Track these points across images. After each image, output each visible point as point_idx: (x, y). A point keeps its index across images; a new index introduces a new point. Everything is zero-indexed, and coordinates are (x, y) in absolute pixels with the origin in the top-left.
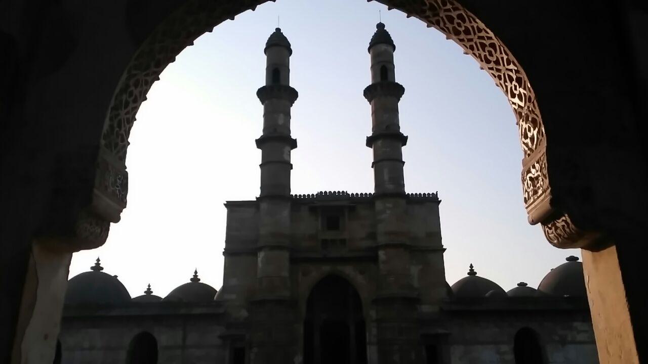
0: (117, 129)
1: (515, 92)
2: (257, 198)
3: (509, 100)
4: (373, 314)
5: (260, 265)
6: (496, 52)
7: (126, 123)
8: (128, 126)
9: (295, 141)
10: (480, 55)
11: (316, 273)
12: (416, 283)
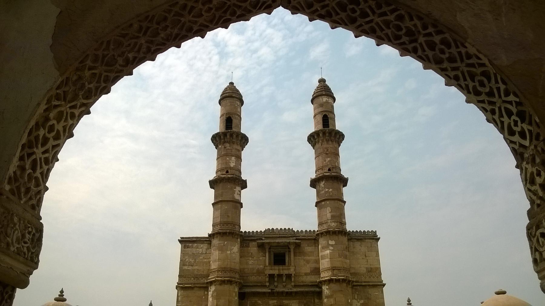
0: (30, 171)
1: (515, 128)
2: (210, 235)
3: (505, 138)
6: (489, 81)
7: (43, 163)
8: (45, 168)
10: (467, 86)
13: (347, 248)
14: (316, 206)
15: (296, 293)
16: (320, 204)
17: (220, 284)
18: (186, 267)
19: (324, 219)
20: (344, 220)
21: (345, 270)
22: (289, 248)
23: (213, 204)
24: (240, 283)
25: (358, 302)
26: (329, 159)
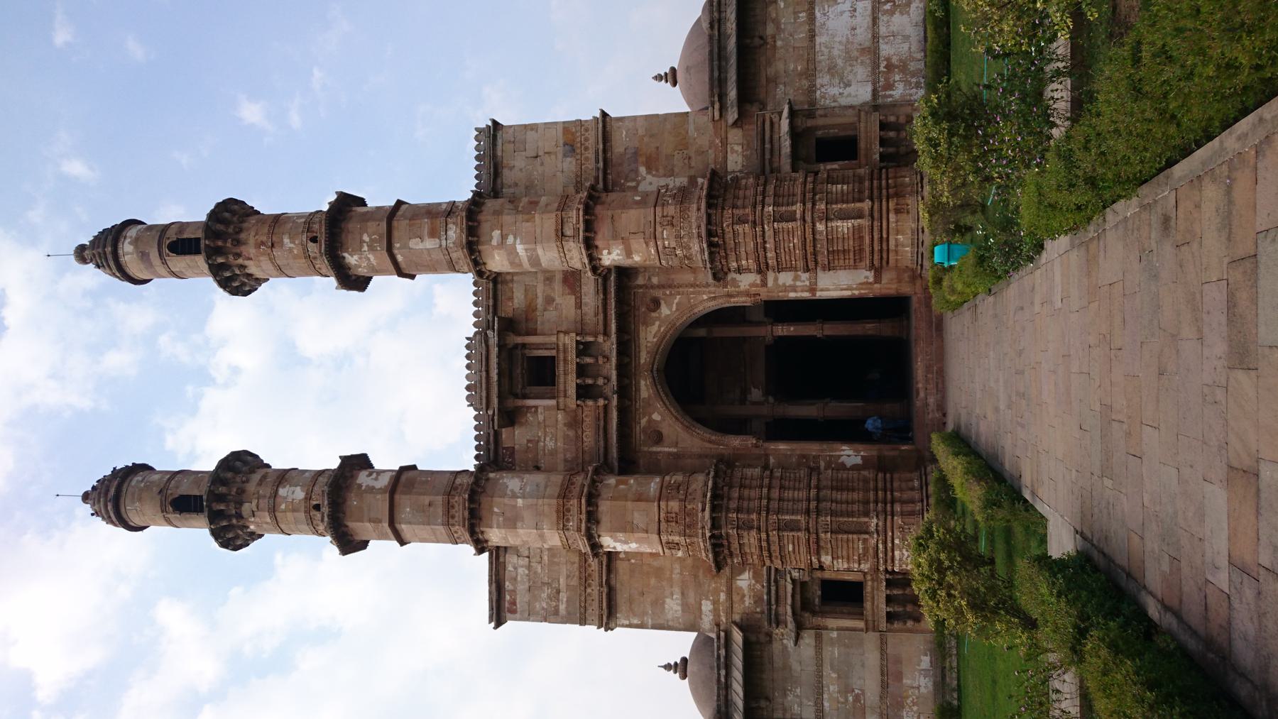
2: (480, 551)
4: (747, 281)
5: (633, 546)
9: (346, 461)
11: (657, 414)
12: (682, 181)
13: (513, 200)
14: (412, 277)
15: (621, 330)
16: (403, 265)
17: (598, 522)
18: (562, 607)
19: (438, 256)
20: (444, 207)
21: (563, 206)
22: (516, 346)
23: (402, 543)
24: (597, 471)
25: (644, 179)
26: (286, 240)
